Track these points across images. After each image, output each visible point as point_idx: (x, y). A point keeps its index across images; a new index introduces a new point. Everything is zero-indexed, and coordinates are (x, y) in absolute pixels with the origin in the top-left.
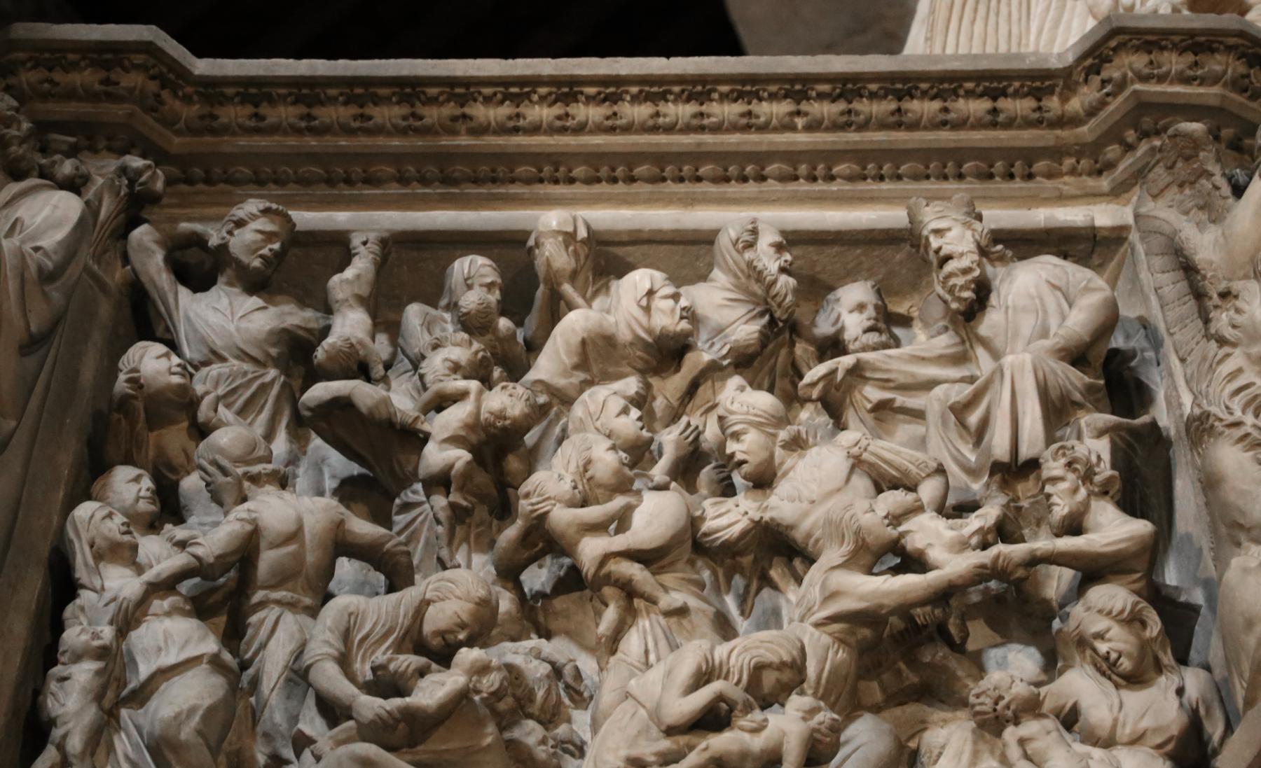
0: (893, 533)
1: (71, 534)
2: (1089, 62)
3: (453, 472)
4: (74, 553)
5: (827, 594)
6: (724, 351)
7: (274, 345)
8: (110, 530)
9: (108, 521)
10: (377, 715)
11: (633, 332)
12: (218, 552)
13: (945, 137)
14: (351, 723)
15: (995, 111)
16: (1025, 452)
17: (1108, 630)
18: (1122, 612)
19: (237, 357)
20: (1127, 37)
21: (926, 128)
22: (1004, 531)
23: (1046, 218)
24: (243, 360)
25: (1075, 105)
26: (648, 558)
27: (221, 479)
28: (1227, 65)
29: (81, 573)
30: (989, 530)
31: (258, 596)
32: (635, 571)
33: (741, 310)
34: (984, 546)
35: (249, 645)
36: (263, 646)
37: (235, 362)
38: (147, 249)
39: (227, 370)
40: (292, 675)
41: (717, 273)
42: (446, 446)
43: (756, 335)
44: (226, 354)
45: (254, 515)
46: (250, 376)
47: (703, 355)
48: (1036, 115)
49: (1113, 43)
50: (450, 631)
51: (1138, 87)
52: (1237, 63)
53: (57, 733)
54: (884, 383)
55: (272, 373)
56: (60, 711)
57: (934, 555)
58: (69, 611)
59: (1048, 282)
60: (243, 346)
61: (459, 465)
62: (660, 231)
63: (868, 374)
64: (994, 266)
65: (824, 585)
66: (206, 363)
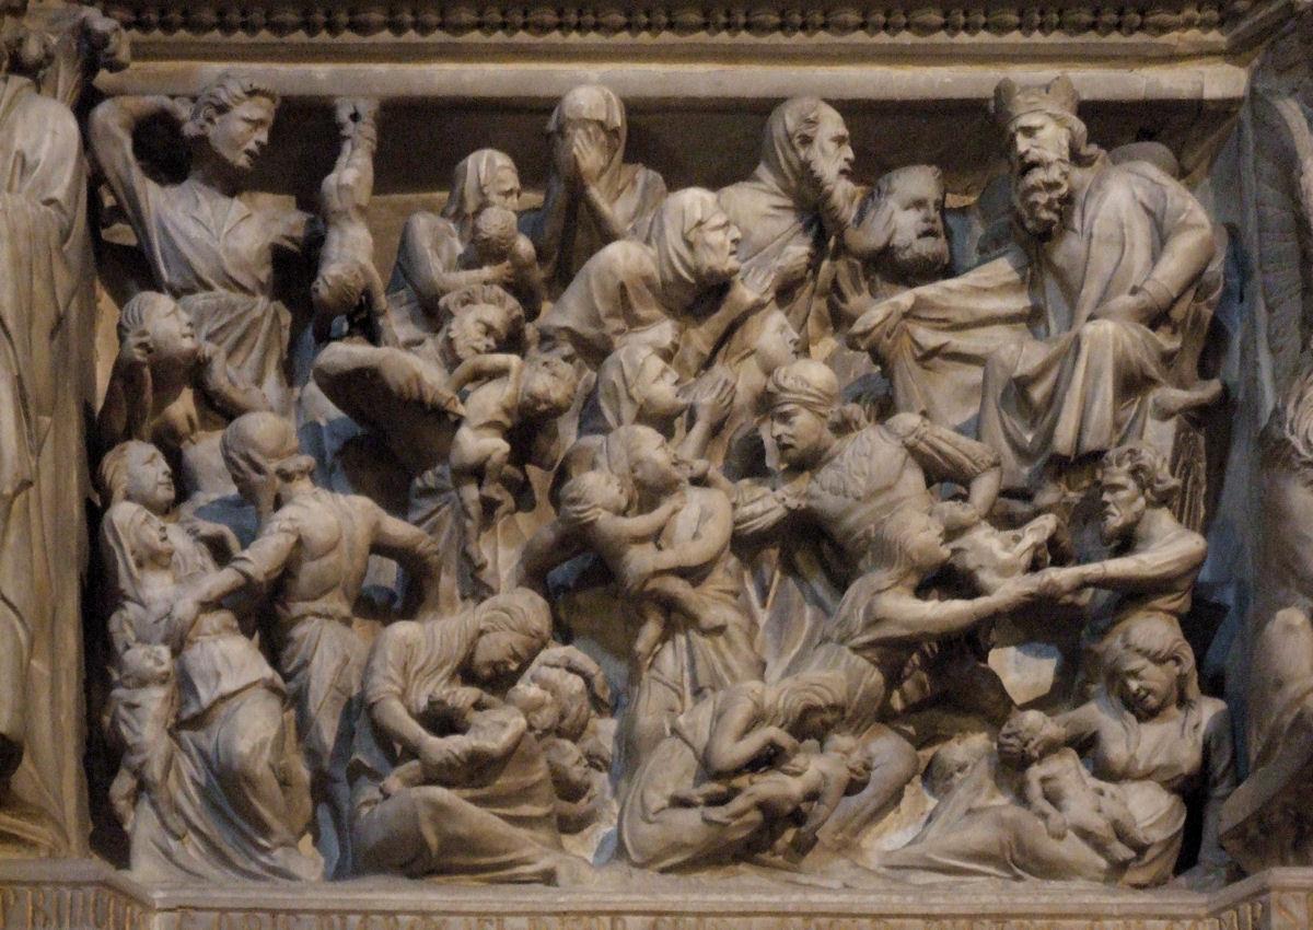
0: (945, 552)
1: (111, 541)
3: (489, 464)
4: (115, 562)
5: (871, 618)
6: (767, 284)
7: (263, 267)
8: (150, 537)
9: (147, 526)
10: (447, 759)
11: (678, 276)
12: (267, 568)
14: (415, 763)
16: (1090, 443)
19: (225, 286)
22: (1055, 552)
24: (232, 290)
26: (694, 574)
27: (256, 477)
29: (125, 584)
31: (298, 608)
32: (677, 587)
33: (788, 221)
34: (1035, 566)
35: (291, 658)
36: (306, 664)
37: (220, 291)
38: (113, 136)
39: (214, 302)
40: (337, 693)
41: (762, 170)
42: (482, 432)
43: (805, 260)
44: (212, 282)
45: (297, 525)
46: (240, 310)
47: (747, 292)
50: (504, 663)
53: (136, 760)
55: (262, 301)
56: (137, 740)
57: (986, 577)
58: (114, 623)
60: (232, 273)
61: (496, 457)
62: (695, 99)
65: (869, 609)
66: (191, 291)
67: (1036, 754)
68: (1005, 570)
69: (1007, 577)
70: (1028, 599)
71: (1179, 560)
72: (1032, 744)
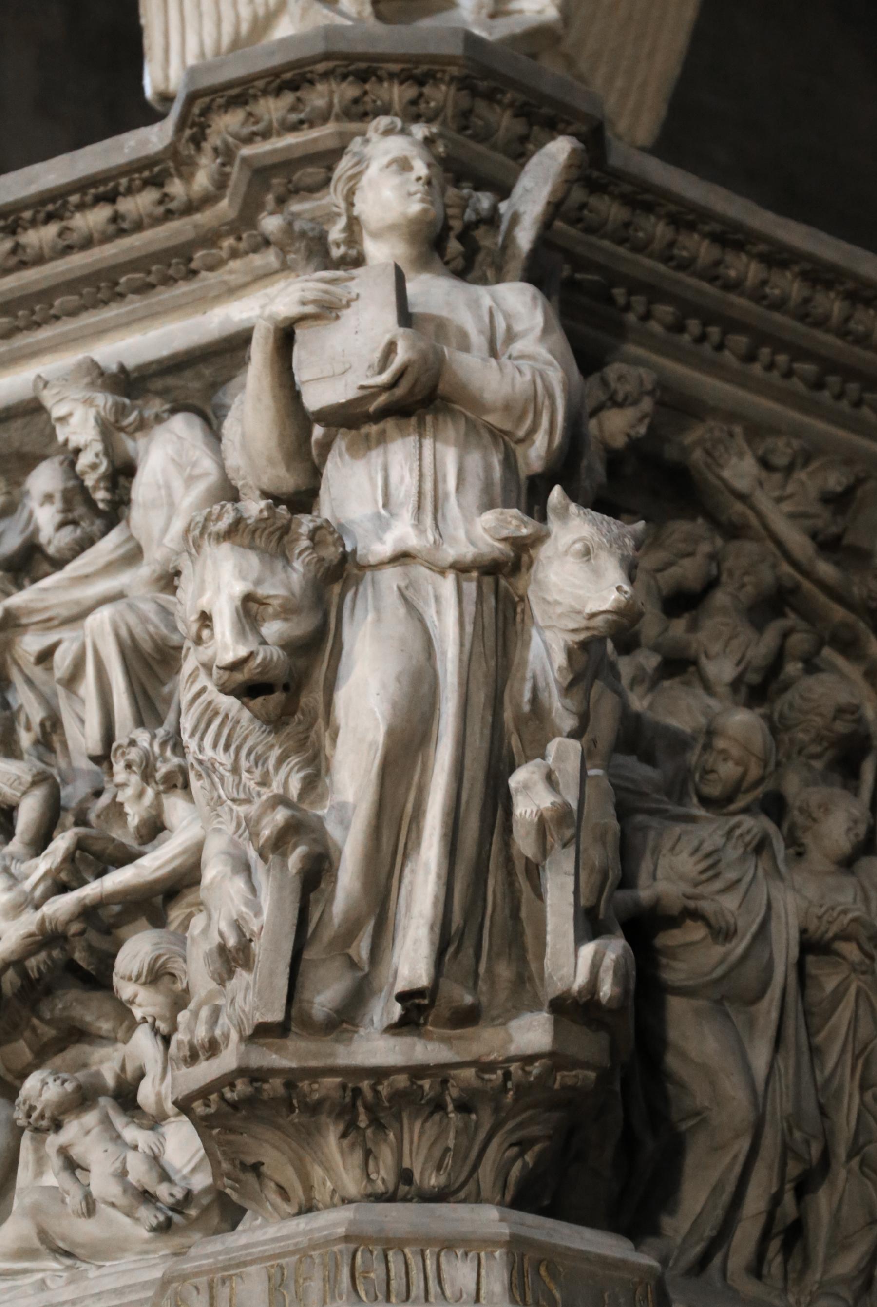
2: (188, 132)
13: (78, 262)
15: (116, 218)
17: (136, 996)
18: (139, 977)
20: (207, 100)
21: (52, 259)
25: (202, 180)
28: (331, 92)
30: (59, 870)
49: (196, 110)
52: (344, 85)
54: (48, 624)
59: (173, 460)
63: (24, 621)
64: (134, 440)
71: (184, 852)
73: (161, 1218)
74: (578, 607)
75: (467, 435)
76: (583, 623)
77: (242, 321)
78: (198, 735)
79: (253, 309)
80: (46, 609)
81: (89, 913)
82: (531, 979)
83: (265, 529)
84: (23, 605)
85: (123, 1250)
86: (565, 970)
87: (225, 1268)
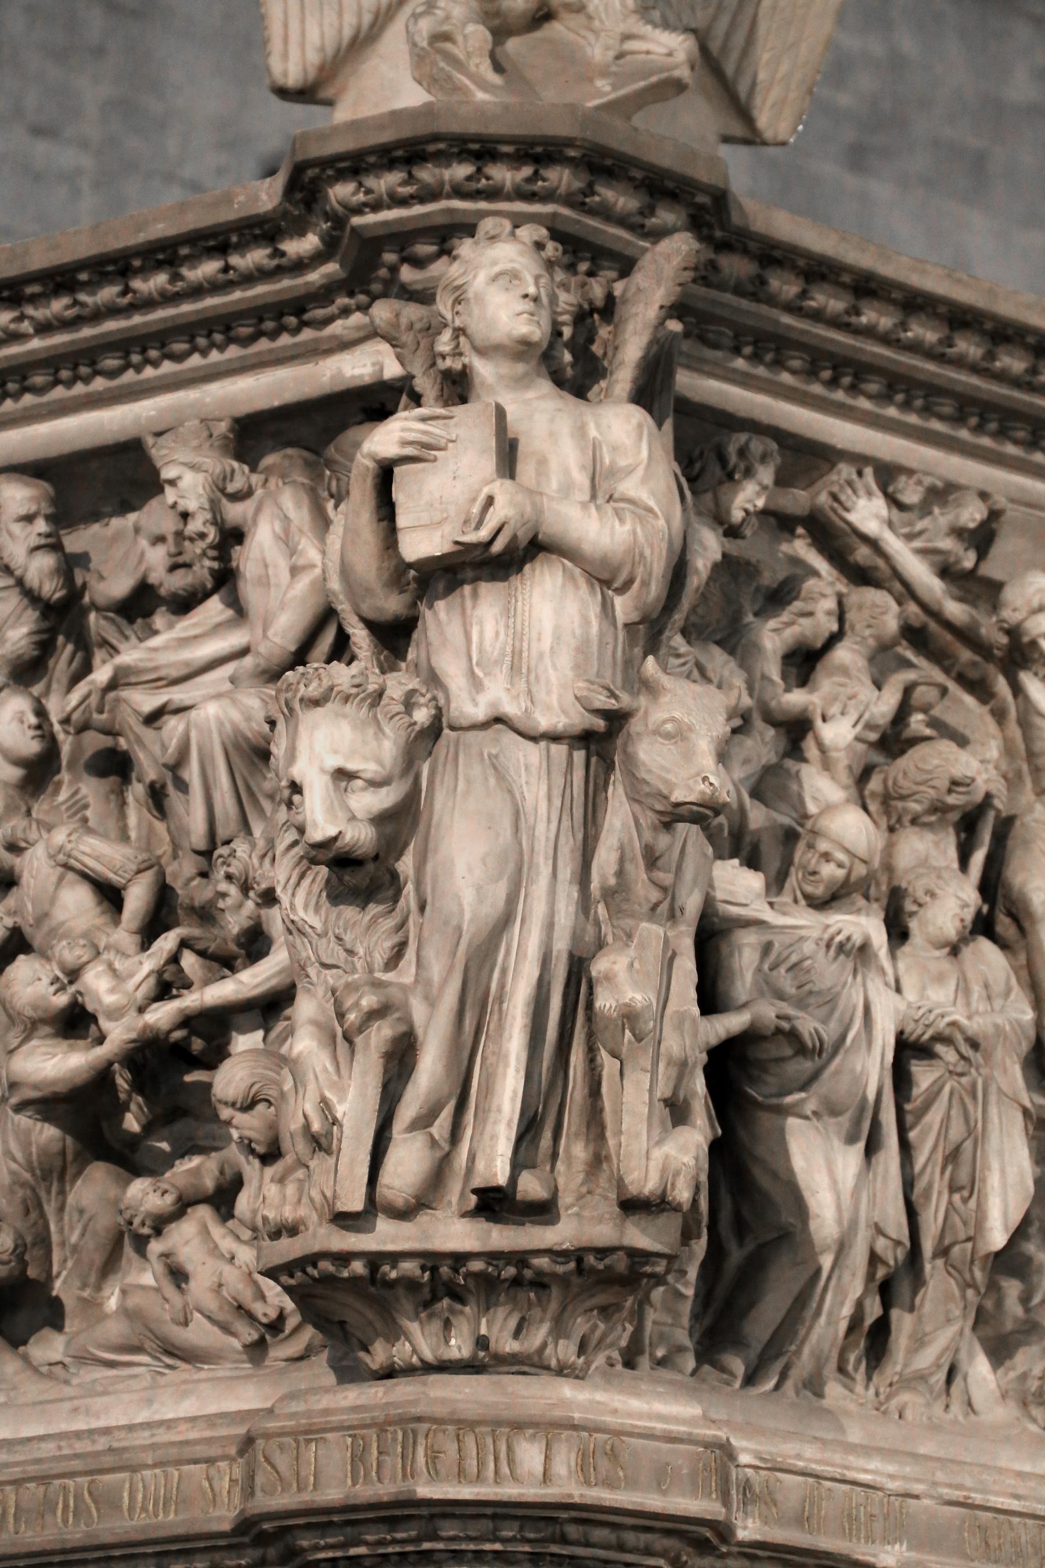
2: (298, 196)
15: (226, 269)
23: (332, 377)
48: (275, 262)
51: (356, 221)
67: (146, 1231)
68: (116, 1013)
69: (117, 1020)
70: (132, 1045)
71: (280, 972)
72: (137, 1221)
73: (255, 1336)
74: (665, 792)
75: (564, 585)
76: (669, 809)
77: (353, 377)
78: (290, 892)
79: (364, 366)
80: (156, 669)
81: (188, 1021)
82: (608, 1158)
83: (358, 694)
84: (133, 664)
85: (220, 1358)
86: (636, 1173)
87: (306, 1432)
